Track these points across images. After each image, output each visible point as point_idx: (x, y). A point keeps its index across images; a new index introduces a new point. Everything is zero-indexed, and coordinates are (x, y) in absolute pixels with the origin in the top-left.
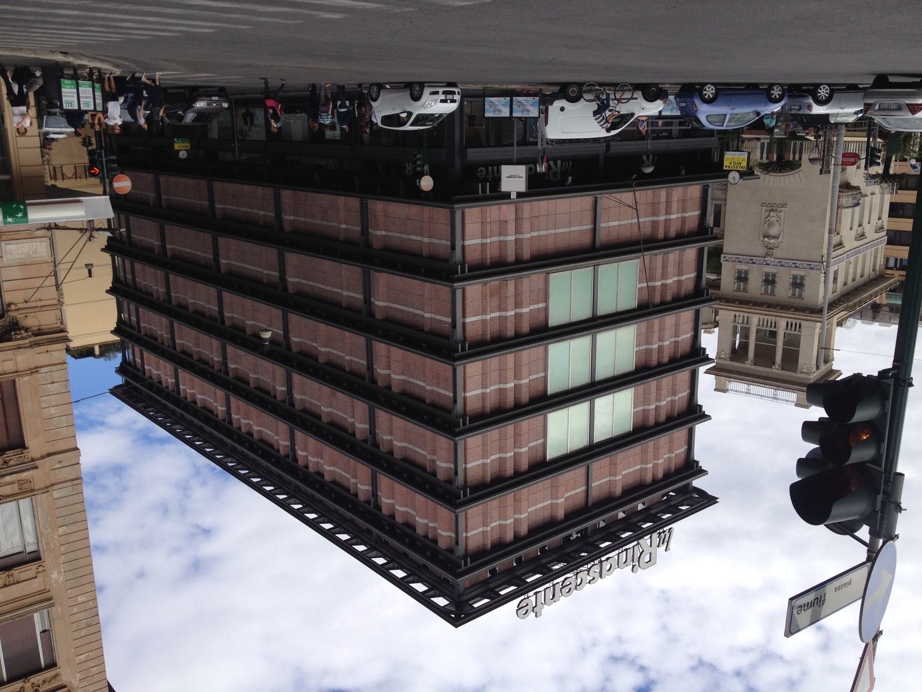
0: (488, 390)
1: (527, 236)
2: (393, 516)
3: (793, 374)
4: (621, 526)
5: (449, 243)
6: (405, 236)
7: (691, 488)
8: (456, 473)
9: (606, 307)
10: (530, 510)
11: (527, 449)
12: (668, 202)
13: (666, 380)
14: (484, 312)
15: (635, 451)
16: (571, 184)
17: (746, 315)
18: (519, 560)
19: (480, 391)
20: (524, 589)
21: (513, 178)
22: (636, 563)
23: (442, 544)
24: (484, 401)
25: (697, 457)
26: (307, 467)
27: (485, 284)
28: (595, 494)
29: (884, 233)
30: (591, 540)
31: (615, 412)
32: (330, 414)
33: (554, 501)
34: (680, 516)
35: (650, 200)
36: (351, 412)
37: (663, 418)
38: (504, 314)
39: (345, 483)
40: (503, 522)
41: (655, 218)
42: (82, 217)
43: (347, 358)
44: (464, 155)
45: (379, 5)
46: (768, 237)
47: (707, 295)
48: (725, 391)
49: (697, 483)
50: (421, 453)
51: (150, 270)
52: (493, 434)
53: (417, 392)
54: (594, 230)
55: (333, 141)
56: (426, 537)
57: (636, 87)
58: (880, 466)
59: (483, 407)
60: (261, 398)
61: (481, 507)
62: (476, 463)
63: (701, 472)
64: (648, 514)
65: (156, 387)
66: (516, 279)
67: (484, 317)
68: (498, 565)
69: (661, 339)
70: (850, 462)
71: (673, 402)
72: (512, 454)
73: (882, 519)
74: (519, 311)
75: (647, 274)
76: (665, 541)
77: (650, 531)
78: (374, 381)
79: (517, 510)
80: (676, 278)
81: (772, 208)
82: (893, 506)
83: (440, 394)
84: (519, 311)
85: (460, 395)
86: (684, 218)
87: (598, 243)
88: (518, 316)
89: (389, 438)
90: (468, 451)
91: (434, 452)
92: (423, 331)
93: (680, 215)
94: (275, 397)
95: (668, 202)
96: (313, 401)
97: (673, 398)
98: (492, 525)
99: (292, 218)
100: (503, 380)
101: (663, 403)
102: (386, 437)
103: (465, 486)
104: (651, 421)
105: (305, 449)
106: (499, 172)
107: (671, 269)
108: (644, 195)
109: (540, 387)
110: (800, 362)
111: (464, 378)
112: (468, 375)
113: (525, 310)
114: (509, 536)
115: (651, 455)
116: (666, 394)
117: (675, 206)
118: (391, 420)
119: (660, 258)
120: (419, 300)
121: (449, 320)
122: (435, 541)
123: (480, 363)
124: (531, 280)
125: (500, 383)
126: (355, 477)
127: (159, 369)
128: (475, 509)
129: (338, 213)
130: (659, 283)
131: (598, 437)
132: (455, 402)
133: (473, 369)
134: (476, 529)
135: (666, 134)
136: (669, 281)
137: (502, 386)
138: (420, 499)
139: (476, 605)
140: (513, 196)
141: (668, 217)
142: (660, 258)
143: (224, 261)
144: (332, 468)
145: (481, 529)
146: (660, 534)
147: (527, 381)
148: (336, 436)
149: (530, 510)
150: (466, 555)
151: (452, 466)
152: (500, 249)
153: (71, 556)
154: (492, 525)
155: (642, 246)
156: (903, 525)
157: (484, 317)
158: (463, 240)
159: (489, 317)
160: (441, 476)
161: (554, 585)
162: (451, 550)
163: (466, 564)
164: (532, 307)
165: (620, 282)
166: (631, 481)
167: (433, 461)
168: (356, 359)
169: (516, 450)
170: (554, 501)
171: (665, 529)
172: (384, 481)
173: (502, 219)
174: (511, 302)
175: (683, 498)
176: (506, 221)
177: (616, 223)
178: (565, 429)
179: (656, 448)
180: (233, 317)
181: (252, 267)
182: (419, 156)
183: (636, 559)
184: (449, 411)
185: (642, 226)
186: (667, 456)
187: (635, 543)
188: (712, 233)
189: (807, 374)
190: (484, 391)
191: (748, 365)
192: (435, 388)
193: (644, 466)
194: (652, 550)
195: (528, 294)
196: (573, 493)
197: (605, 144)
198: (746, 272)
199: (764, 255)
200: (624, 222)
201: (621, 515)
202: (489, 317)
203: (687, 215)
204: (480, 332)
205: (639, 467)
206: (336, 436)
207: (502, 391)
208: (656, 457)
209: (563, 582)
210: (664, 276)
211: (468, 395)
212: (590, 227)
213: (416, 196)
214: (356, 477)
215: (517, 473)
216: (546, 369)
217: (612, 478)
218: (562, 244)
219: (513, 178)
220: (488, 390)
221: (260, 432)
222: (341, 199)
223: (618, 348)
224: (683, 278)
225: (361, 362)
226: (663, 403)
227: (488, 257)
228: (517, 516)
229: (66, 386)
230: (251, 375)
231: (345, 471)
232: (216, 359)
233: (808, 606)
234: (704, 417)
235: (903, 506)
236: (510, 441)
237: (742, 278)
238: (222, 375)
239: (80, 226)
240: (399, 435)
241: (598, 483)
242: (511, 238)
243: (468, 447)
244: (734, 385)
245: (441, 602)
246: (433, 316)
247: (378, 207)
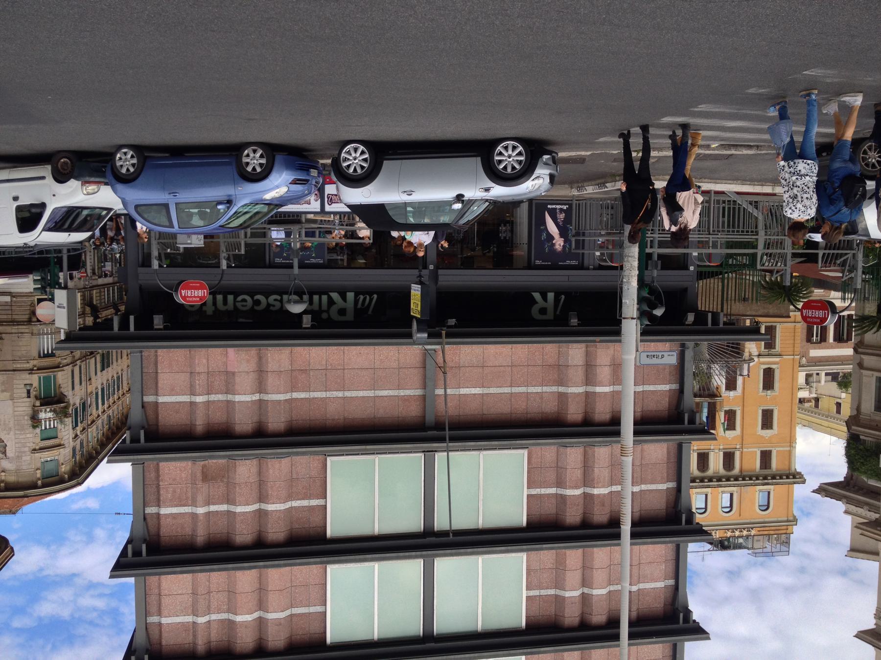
0: (201, 620)
1: (281, 397)
14: (194, 504)
24: (195, 636)
38: (232, 508)
41: (561, 389)
74: (264, 506)
84: (264, 506)
111: (160, 595)
123: (189, 576)
124: (282, 466)
135: (574, 263)
137: (232, 617)
141: (590, 389)
152: (228, 412)
155: (447, 433)
159: (201, 511)
173: (230, 369)
176: (233, 373)
210: (587, 480)
218: (359, 413)
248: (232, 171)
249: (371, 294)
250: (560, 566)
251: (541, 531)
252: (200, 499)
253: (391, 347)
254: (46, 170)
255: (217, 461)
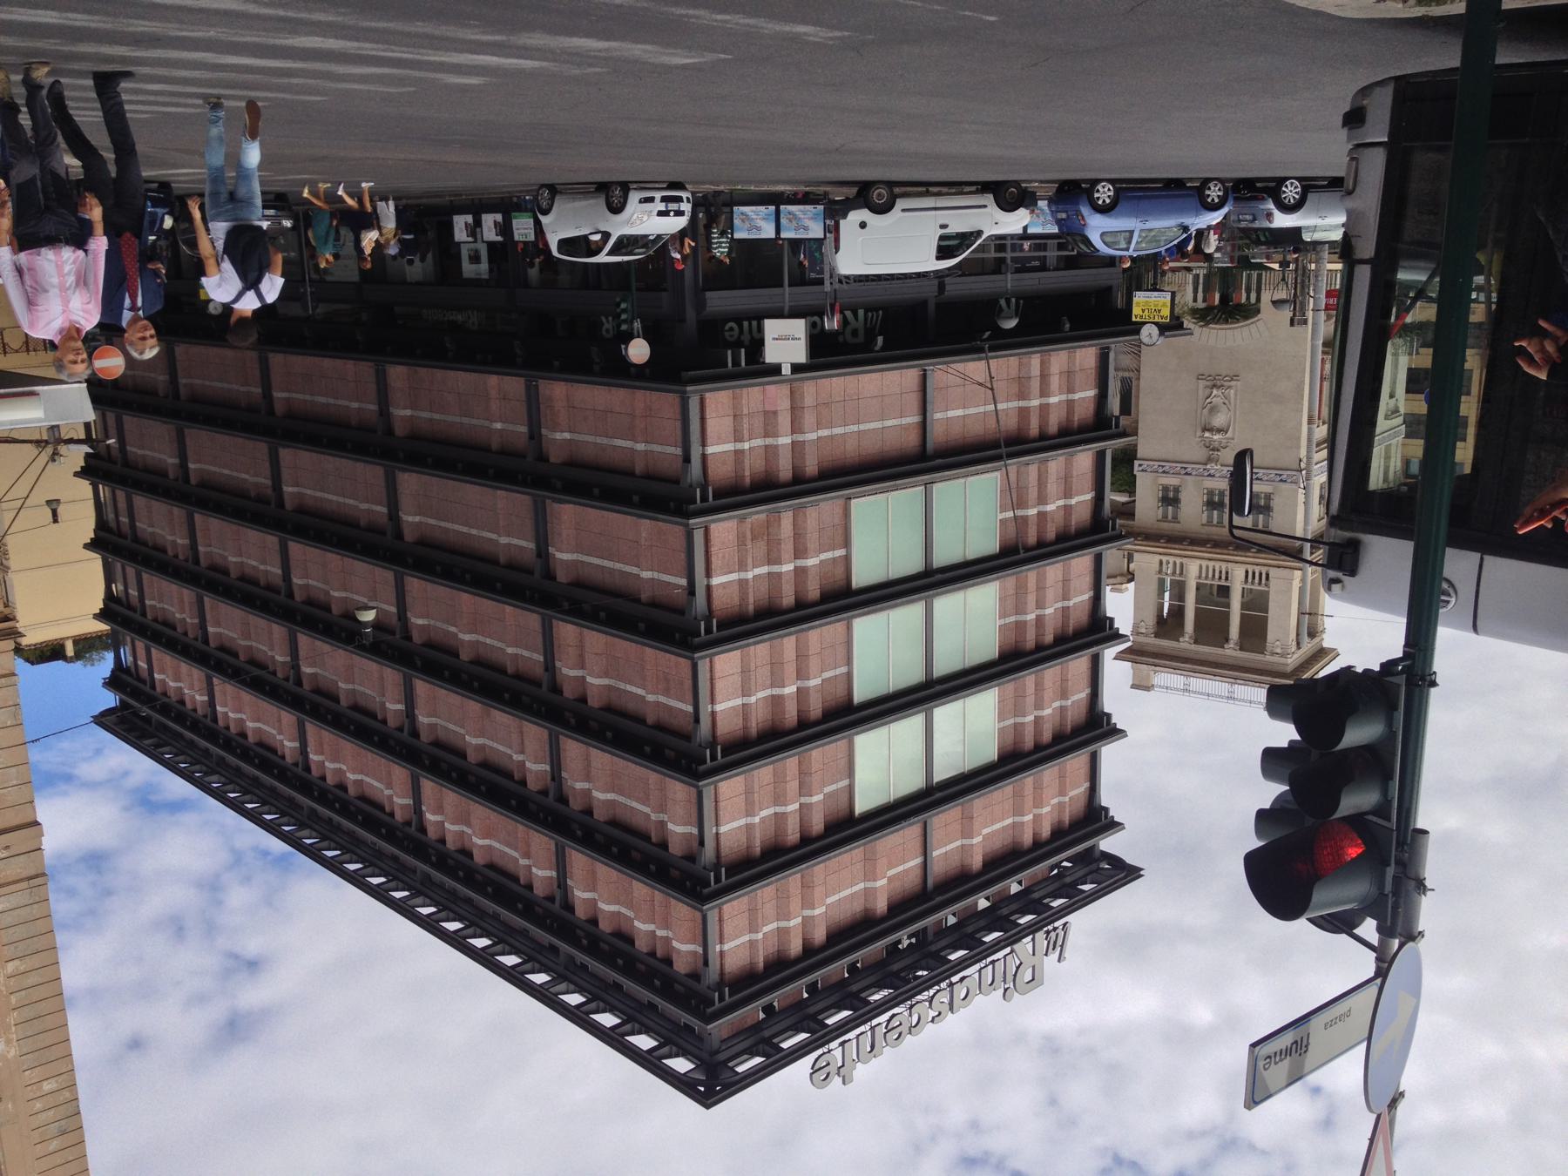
1: (812, 436)
2: (594, 921)
3: (1259, 657)
4: (982, 923)
5: (679, 451)
6: (605, 441)
7: (1097, 854)
8: (702, 843)
9: (946, 553)
10: (829, 900)
11: (821, 797)
12: (1044, 377)
13: (1051, 673)
14: (742, 567)
15: (1002, 794)
16: (883, 349)
17: (1178, 561)
18: (812, 988)
19: (739, 701)
20: (822, 1036)
21: (785, 341)
22: (1011, 985)
23: (681, 967)
24: (746, 718)
25: (1105, 799)
26: (443, 841)
27: (742, 519)
28: (938, 869)
29: (1400, 420)
30: (933, 948)
31: (968, 729)
32: (482, 748)
33: (870, 884)
34: (1079, 901)
35: (1014, 373)
36: (519, 745)
37: (1047, 736)
38: (775, 569)
39: (510, 867)
40: (783, 924)
41: (1022, 404)
42: (39, 420)
43: (510, 650)
44: (700, 304)
45: (544, 64)
46: (1210, 430)
47: (1114, 528)
48: (1148, 688)
49: (1108, 844)
50: (641, 810)
51: (159, 508)
52: (763, 773)
53: (631, 706)
54: (923, 425)
55: (476, 282)
56: (652, 954)
57: (985, 187)
58: (1389, 819)
59: (745, 728)
60: (361, 726)
61: (745, 899)
62: (735, 824)
63: (1112, 825)
64: (1027, 901)
65: (175, 710)
66: (796, 509)
67: (743, 575)
68: (776, 999)
69: (1040, 604)
70: (1338, 815)
71: (1063, 709)
72: (796, 806)
73: (1396, 907)
74: (800, 563)
75: (1014, 497)
76: (1057, 945)
77: (1032, 929)
78: (556, 689)
79: (808, 903)
80: (1061, 503)
81: (1215, 382)
82: (1412, 884)
83: (670, 709)
84: (800, 563)
85: (705, 710)
86: (1070, 403)
87: (930, 446)
88: (800, 572)
89: (586, 785)
90: (722, 805)
91: (662, 808)
92: (637, 601)
93: (1064, 397)
94: (384, 722)
95: (1044, 377)
96: (452, 727)
97: (1064, 703)
98: (766, 929)
99: (408, 412)
100: (777, 681)
101: (1048, 711)
102: (579, 785)
103: (717, 866)
104: (1029, 743)
105: (439, 810)
106: (761, 329)
107: (1053, 487)
108: (1004, 365)
109: (841, 692)
110: (1270, 637)
111: (712, 679)
112: (717, 674)
113: (811, 562)
114: (795, 947)
115: (1029, 801)
116: (1052, 695)
117: (1055, 381)
118: (587, 759)
119: (1033, 470)
120: (630, 551)
121: (684, 582)
122: (669, 962)
124: (820, 511)
125: (772, 686)
126: (527, 855)
127: (180, 680)
128: (735, 903)
129: (487, 403)
130: (1033, 512)
131: (940, 775)
132: (697, 720)
133: (726, 664)
134: (738, 937)
135: (1037, 263)
136: (1050, 508)
137: (776, 691)
138: (640, 889)
139: (740, 1069)
140: (786, 370)
141: (1045, 401)
142: (1033, 470)
143: (290, 489)
144: (487, 842)
145: (746, 938)
146: (1048, 932)
147: (818, 681)
148: (493, 786)
149: (829, 900)
150: (721, 983)
151: (695, 831)
153: (28, 1013)
154: (766, 929)
156: (1429, 913)
157: (743, 575)
158: (704, 444)
159: (750, 575)
160: (676, 849)
161: (872, 1028)
162: (695, 976)
163: (721, 999)
164: (824, 556)
165: (970, 512)
166: (997, 844)
167: (662, 824)
168: (526, 653)
169: (803, 800)
170: (870, 884)
171: (1056, 924)
172: (579, 860)
174: (787, 548)
175: (1086, 870)
176: (775, 413)
177: (959, 412)
178: (883, 763)
179: (1038, 787)
180: (307, 586)
181: (341, 499)
182: (623, 306)
183: (1010, 977)
184: (687, 737)
185: (1002, 417)
186: (1055, 801)
187: (1008, 950)
188: (1117, 426)
189: (1282, 655)
190: (746, 700)
191: (1185, 644)
192: (662, 699)
193: (1018, 819)
194: (1035, 960)
195: (816, 535)
196: (901, 868)
197: (936, 282)
198: (1177, 490)
199: (1202, 458)
200: (972, 411)
201: (983, 904)
202: (750, 575)
203: (1077, 396)
204: (736, 601)
205: (1009, 821)
206: (493, 786)
207: (777, 701)
208: (1038, 803)
209: (889, 1021)
210: (1042, 500)
211: (719, 707)
212: (914, 419)
213: (620, 372)
214: (530, 855)
215: (805, 840)
216: (849, 661)
217: (966, 842)
218: (871, 448)
219: (785, 341)
220: (753, 699)
221: (359, 783)
222: (493, 380)
223: (971, 621)
224: (1073, 502)
225: (534, 657)
226: (1048, 711)
227: (747, 473)
228: (808, 913)
229: (15, 716)
230: (342, 685)
231: (508, 845)
232: (279, 658)
233: (1283, 1055)
234: (1114, 733)
235: (1428, 884)
236: (793, 786)
237: (1170, 499)
238: (290, 685)
239: (37, 437)
240: (602, 780)
241: (943, 850)
242: (785, 440)
243: (721, 798)
244: (1165, 678)
245: (681, 1065)
246: (656, 575)
247: (557, 391)
248: (1195, 201)
249: (877, 310)
250: (1021, 591)
251: (1011, 557)
252: (750, 561)
253: (873, 375)
254: (988, 199)
255: (757, 516)
